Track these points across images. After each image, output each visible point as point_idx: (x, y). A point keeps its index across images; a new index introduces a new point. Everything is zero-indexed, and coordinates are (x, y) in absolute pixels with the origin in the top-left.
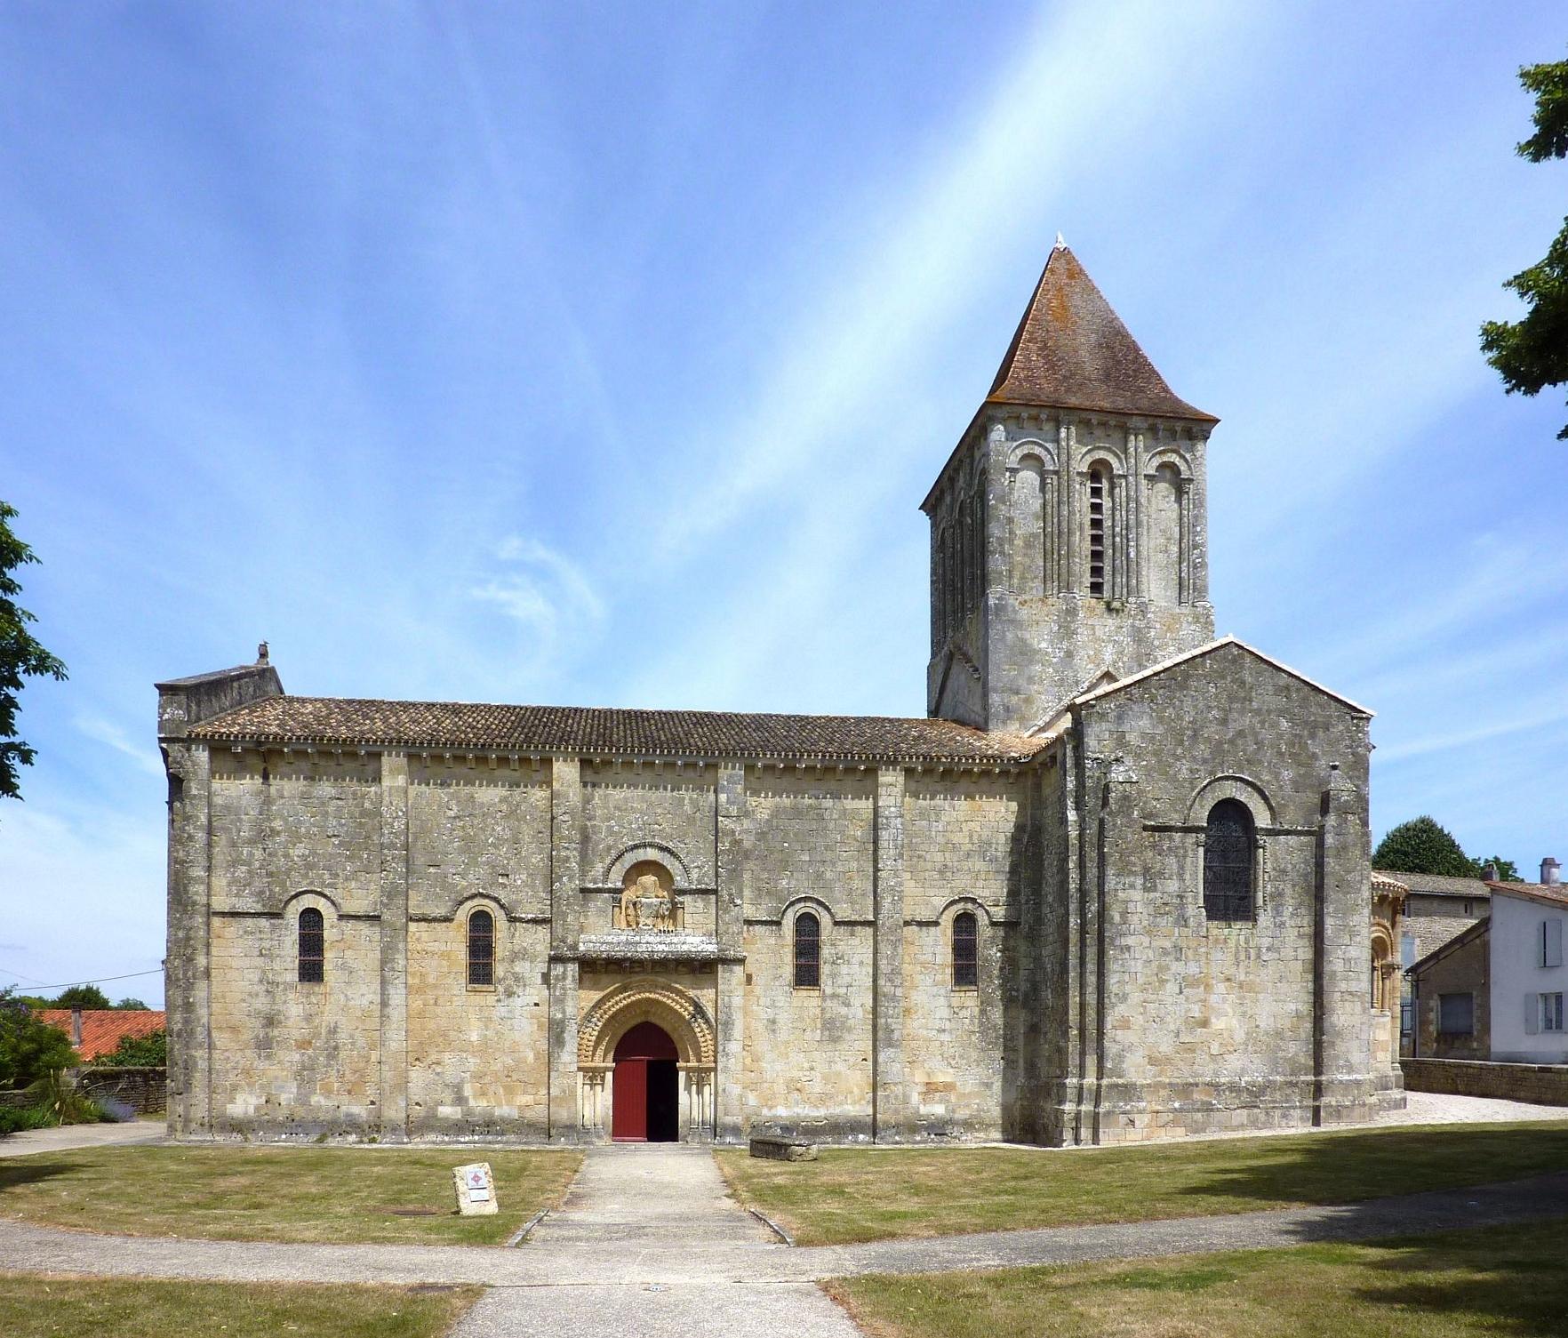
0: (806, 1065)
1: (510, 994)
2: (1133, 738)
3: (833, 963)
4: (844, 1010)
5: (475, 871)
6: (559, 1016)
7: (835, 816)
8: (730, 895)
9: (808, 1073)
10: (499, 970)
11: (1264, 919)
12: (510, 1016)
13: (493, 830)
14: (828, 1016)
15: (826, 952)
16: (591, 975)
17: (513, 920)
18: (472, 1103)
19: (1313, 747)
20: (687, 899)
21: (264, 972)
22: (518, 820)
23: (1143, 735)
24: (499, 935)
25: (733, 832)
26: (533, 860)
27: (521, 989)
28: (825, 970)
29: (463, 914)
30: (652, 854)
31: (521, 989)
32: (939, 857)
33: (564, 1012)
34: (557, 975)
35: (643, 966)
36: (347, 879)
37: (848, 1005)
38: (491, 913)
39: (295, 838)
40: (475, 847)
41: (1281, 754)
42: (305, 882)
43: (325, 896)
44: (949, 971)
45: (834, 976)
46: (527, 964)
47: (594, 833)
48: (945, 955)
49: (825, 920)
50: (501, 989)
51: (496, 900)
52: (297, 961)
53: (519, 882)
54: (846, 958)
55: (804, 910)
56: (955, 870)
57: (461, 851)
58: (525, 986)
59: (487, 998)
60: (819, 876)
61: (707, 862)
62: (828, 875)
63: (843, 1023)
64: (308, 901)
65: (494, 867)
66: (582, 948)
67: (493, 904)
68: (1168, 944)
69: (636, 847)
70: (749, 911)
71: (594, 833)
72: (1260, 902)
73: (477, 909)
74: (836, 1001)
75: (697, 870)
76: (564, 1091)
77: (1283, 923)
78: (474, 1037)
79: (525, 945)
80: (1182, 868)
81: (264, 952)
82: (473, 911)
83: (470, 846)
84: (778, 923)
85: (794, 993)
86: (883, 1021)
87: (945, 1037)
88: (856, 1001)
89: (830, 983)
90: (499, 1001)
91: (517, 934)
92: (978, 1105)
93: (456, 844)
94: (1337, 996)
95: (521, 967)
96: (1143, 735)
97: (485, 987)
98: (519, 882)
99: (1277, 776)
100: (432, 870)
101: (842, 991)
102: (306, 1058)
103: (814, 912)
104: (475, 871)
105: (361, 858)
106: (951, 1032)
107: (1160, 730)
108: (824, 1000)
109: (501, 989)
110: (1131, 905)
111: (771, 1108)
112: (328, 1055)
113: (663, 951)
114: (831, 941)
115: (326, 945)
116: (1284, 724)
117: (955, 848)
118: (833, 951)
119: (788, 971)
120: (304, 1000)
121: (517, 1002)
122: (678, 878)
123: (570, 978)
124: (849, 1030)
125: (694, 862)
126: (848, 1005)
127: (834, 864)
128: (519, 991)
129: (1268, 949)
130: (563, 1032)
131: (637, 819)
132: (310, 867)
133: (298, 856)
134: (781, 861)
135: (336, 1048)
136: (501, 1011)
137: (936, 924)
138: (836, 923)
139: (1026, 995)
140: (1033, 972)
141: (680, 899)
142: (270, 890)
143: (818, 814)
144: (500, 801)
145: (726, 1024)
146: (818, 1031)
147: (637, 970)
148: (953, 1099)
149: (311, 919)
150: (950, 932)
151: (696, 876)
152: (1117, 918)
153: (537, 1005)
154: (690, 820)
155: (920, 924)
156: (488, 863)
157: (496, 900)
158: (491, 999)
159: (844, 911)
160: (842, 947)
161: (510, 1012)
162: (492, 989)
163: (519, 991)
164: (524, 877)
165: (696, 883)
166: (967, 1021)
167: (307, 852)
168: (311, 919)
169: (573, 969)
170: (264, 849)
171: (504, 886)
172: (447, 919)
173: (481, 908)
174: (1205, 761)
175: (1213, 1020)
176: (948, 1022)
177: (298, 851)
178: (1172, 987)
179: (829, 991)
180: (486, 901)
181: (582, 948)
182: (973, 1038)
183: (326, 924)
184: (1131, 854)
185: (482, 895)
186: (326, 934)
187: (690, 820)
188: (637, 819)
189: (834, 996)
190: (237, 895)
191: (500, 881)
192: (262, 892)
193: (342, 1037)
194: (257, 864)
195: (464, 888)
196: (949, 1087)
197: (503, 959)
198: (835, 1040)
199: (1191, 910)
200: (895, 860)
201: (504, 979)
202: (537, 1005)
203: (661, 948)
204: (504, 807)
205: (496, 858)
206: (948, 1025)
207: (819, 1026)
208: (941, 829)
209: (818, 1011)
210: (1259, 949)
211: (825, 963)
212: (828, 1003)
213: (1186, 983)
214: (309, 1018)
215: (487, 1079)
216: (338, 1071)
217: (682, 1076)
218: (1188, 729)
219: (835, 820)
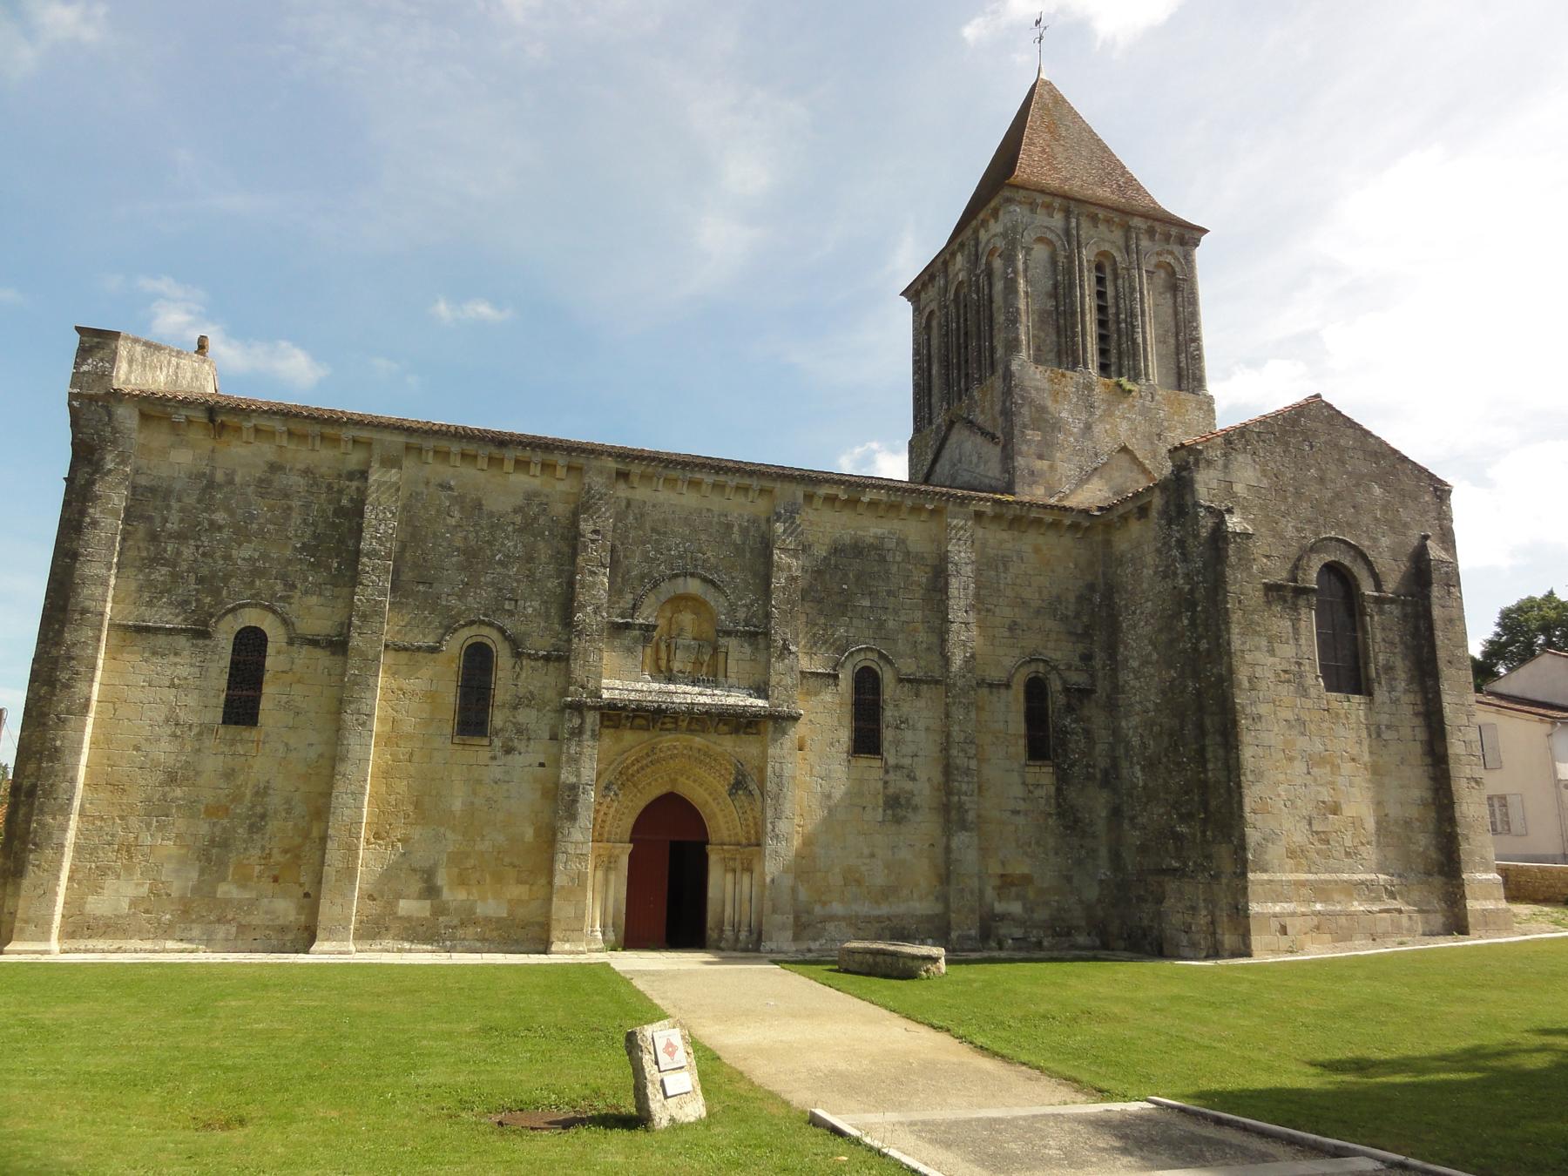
0: (866, 851)
1: (509, 751)
2: (1239, 488)
3: (897, 727)
4: (909, 785)
5: (475, 593)
6: (573, 779)
7: (898, 559)
8: (784, 640)
9: (867, 861)
10: (498, 718)
11: (1381, 694)
12: (506, 779)
13: (503, 544)
14: (891, 791)
15: (889, 714)
16: (612, 730)
17: (518, 655)
18: (446, 894)
19: (1404, 515)
20: (732, 643)
21: (172, 709)
22: (535, 536)
23: (1250, 487)
24: (500, 674)
25: (790, 567)
26: (549, 585)
27: (524, 743)
28: (888, 735)
29: (455, 645)
30: (694, 586)
31: (524, 743)
32: (1007, 611)
33: (578, 776)
34: (573, 728)
35: (676, 723)
36: (306, 592)
37: (914, 779)
38: (493, 646)
39: (242, 534)
40: (478, 563)
41: (1377, 519)
42: (249, 593)
43: (274, 612)
44: (1022, 742)
45: (897, 743)
46: (534, 712)
47: (626, 557)
48: (1018, 725)
49: (887, 676)
50: (497, 742)
51: (502, 631)
52: (223, 696)
53: (530, 610)
54: (911, 722)
55: (864, 664)
56: (1025, 628)
57: (462, 568)
58: (529, 739)
59: (479, 753)
60: (881, 625)
61: (757, 600)
62: (891, 624)
63: (908, 800)
64: (251, 618)
65: (500, 590)
66: (606, 695)
67: (495, 635)
68: (1291, 717)
69: (677, 576)
70: (805, 664)
71: (626, 557)
72: (1373, 674)
73: (474, 640)
74: (899, 773)
75: (745, 609)
76: (573, 879)
77: (1398, 699)
78: (457, 806)
79: (531, 688)
80: (1296, 630)
81: (176, 681)
82: (470, 642)
83: (471, 558)
84: (836, 677)
85: (853, 761)
86: (956, 798)
87: (1020, 820)
88: (922, 774)
89: (893, 751)
90: (494, 758)
91: (523, 675)
92: (1057, 902)
93: (454, 559)
94: (1464, 783)
95: (526, 716)
96: (1250, 487)
97: (476, 740)
98: (530, 610)
99: (1375, 540)
100: (421, 588)
101: (907, 761)
102: (218, 831)
103: (874, 666)
104: (475, 593)
105: (328, 568)
106: (1026, 814)
107: (1265, 483)
108: (887, 772)
109: (497, 742)
110: (1258, 669)
111: (824, 904)
112: (252, 826)
113: (705, 704)
114: (896, 702)
115: (267, 677)
116: (1377, 491)
117: (1024, 603)
118: (896, 714)
119: (845, 736)
120: (226, 750)
121: (517, 760)
122: (723, 617)
123: (589, 733)
124: (915, 809)
125: (741, 599)
126: (914, 779)
127: (896, 612)
128: (520, 746)
129: (1388, 727)
130: (575, 801)
131: (677, 545)
132: (257, 573)
133: (244, 559)
134: (839, 605)
135: (263, 817)
136: (496, 771)
137: (1008, 686)
138: (901, 680)
139: (1106, 773)
140: (1112, 747)
141: (722, 641)
142: (197, 600)
143: (879, 555)
144: (515, 511)
145: (777, 797)
146: (880, 810)
147: (669, 726)
148: (1031, 894)
149: (250, 645)
150: (1021, 697)
151: (744, 615)
152: (1246, 684)
153: (542, 765)
154: (739, 550)
155: (991, 685)
156: (492, 584)
157: (502, 631)
158: (484, 755)
159: (908, 666)
160: (905, 708)
161: (507, 772)
162: (486, 742)
163: (520, 746)
164: (536, 604)
165: (743, 624)
166: (1043, 801)
167: (256, 555)
168: (250, 645)
169: (592, 719)
170: (197, 547)
171: (511, 614)
172: (433, 650)
173: (479, 639)
174: (1310, 521)
175: (1344, 806)
176: (1021, 802)
177: (244, 552)
178: (1299, 767)
179: (892, 761)
180: (486, 631)
181: (606, 695)
182: (1050, 821)
183: (271, 649)
184: (1253, 612)
185: (482, 623)
186: (269, 662)
187: (739, 550)
188: (677, 545)
189: (898, 767)
190: (150, 604)
191: (507, 607)
192: (187, 602)
193: (275, 801)
194: (184, 566)
195: (460, 614)
196: (1027, 879)
197: (503, 706)
198: (898, 821)
199: (1310, 680)
200: (966, 612)
201: (502, 730)
202: (542, 765)
203: (702, 699)
204: (518, 519)
205: (504, 580)
206: (1022, 806)
207: (881, 802)
208: (1009, 581)
209: (880, 785)
210: (1379, 727)
211: (887, 727)
212: (892, 776)
213: (1313, 761)
214: (229, 775)
215: (471, 862)
216: (263, 848)
217: (713, 858)
218: (1289, 485)
219: (898, 563)
